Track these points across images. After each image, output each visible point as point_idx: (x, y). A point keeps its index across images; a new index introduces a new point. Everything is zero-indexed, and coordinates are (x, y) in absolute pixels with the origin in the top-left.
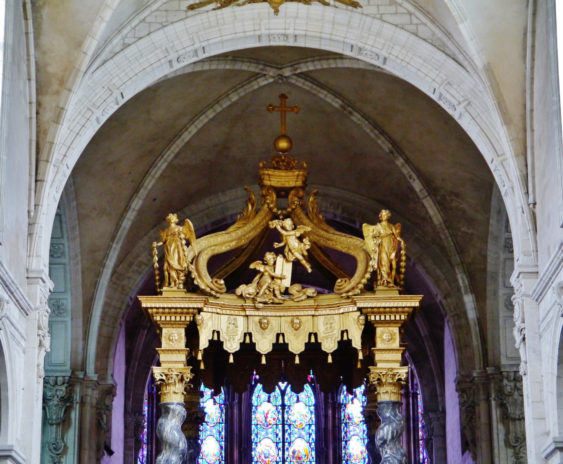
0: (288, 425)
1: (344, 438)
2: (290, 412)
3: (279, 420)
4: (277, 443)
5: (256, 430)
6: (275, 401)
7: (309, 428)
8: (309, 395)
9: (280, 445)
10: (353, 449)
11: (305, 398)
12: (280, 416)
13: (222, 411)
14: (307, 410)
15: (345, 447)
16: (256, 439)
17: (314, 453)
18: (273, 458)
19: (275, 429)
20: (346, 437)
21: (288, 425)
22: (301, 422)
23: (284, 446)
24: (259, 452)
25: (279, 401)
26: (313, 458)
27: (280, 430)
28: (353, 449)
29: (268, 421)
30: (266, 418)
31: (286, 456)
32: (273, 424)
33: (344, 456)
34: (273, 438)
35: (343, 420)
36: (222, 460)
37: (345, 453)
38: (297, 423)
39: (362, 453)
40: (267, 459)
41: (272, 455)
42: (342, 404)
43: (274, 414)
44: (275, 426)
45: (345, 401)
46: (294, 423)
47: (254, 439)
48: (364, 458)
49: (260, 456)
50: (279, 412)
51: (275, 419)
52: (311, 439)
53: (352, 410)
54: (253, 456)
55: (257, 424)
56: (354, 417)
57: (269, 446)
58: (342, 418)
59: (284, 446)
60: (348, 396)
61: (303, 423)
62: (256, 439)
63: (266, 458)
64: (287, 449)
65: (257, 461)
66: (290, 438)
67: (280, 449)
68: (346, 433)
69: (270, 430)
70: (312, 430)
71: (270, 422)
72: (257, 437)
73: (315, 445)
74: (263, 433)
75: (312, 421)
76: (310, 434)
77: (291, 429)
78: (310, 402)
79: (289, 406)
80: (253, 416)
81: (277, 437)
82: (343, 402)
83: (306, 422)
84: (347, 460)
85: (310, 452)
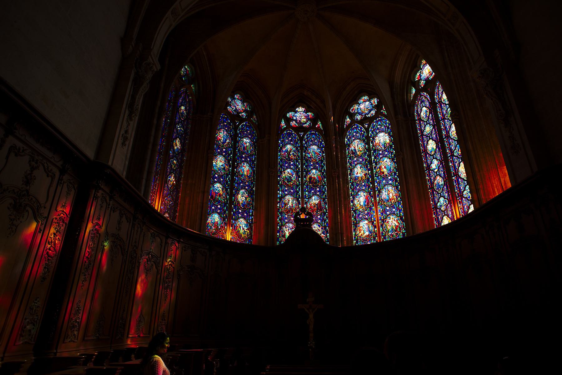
1: (349, 167)
3: (299, 157)
4: (297, 174)
9: (300, 174)
10: (357, 174)
12: (299, 154)
13: (255, 148)
15: (350, 174)
18: (294, 182)
19: (296, 163)
20: (351, 167)
23: (302, 174)
24: (283, 178)
25: (298, 144)
26: (325, 183)
28: (357, 174)
29: (290, 156)
30: (289, 154)
33: (350, 180)
35: (348, 155)
36: (254, 181)
37: (351, 178)
39: (365, 175)
42: (347, 144)
43: (295, 152)
45: (348, 142)
47: (279, 169)
48: (368, 179)
49: (284, 181)
50: (298, 151)
52: (323, 170)
53: (355, 148)
55: (282, 159)
56: (357, 151)
58: (347, 154)
59: (302, 174)
60: (351, 139)
61: (317, 159)
63: (288, 182)
64: (305, 177)
68: (350, 164)
69: (292, 163)
70: (324, 164)
74: (287, 165)
75: (324, 158)
76: (323, 167)
79: (306, 148)
82: (347, 143)
84: (353, 182)
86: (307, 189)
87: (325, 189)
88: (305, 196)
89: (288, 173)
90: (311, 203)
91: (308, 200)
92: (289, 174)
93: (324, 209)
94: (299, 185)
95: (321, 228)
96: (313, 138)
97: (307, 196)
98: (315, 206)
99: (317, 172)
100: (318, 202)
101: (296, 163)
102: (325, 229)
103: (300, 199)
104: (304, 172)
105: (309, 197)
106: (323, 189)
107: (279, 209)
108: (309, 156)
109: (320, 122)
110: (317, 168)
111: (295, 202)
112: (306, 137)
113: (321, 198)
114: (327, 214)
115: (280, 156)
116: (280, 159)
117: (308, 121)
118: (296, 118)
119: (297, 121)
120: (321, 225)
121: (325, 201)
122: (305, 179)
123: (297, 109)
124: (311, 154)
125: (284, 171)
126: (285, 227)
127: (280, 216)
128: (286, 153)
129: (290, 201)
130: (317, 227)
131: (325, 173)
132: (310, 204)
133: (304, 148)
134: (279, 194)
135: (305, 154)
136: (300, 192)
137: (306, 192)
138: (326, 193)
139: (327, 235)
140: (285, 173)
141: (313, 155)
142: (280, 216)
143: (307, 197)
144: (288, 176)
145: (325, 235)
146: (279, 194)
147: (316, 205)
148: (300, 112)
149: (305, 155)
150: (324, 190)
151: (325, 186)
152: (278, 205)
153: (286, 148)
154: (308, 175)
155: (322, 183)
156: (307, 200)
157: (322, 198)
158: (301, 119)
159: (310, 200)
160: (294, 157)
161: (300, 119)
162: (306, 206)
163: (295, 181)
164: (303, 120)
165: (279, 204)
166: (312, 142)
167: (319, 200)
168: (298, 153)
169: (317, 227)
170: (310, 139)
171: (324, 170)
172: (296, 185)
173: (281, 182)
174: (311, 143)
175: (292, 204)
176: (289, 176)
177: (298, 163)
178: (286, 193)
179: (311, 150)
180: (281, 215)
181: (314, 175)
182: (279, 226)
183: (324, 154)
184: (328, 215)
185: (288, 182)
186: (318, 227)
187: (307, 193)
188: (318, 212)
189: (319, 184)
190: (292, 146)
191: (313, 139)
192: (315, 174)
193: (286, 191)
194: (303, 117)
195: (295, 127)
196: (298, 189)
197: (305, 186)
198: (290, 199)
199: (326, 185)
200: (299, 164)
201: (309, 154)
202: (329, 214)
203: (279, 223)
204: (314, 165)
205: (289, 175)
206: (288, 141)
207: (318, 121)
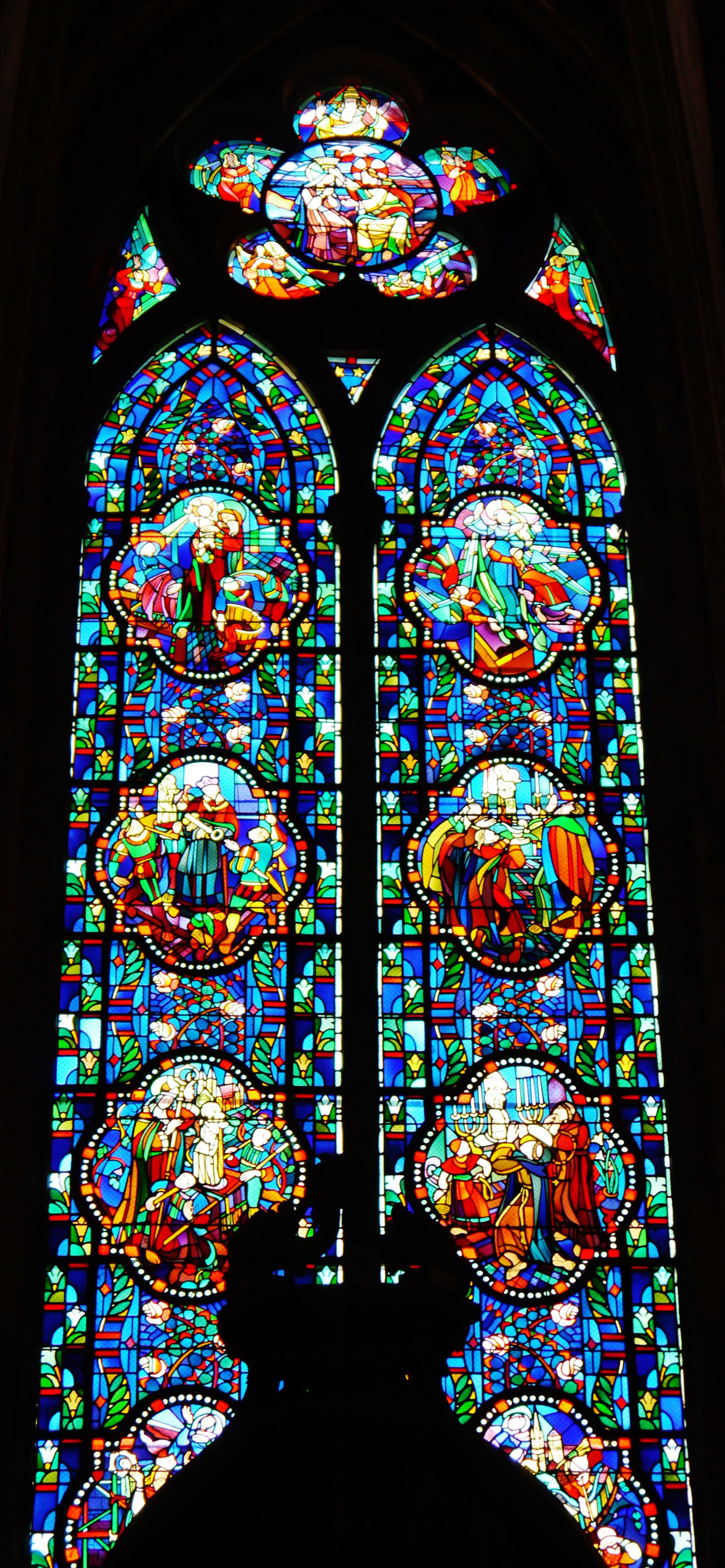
0: (396, 653)
2: (415, 563)
3: (323, 624)
5: (108, 694)
6: (284, 478)
7: (594, 684)
8: (579, 442)
11: (543, 467)
14: (565, 552)
16: (104, 759)
17: (638, 872)
18: (258, 906)
19: (284, 686)
21: (396, 653)
22: (522, 635)
24: (128, 865)
25: (318, 486)
26: (635, 912)
27: (329, 690)
29: (221, 623)
31: (381, 894)
32: (260, 644)
34: (257, 751)
38: (479, 643)
40: (208, 918)
41: (245, 881)
43: (280, 574)
44: (276, 666)
46: (453, 645)
47: (88, 759)
51: (290, 607)
52: (609, 765)
54: (70, 891)
55: (122, 646)
57: (231, 811)
61: (540, 642)
62: (104, 759)
63: (187, 906)
65: (109, 936)
66: (418, 751)
67: (326, 837)
69: (237, 692)
70: (622, 698)
71: (243, 635)
72: (114, 743)
73: (647, 809)
74: (174, 714)
75: (619, 631)
77: (432, 686)
78: (593, 497)
80: (90, 589)
81: (297, 746)
83: (564, 638)
85: (603, 863)
86: (413, 988)
87: (638, 984)
88: (399, 1059)
89: (195, 805)
90: (464, 1149)
91: (431, 1120)
92: (209, 817)
93: (625, 1226)
94: (315, 941)
95: (592, 1455)
96: (494, 413)
97: (415, 1063)
98: (512, 1186)
99: (543, 785)
100: (547, 1135)
101: (284, 686)
102: (641, 1469)
103: (324, 1109)
104: (386, 786)
105: (439, 1075)
106: (612, 974)
107: (64, 1228)
108: (445, 613)
109: (572, 251)
110: (545, 744)
111: (261, 1136)
112: (408, 408)
113: (585, 1089)
114: (662, 1276)
115: (96, 616)
116: (94, 647)
117: (429, 238)
118: (300, 209)
119: (308, 233)
120: (595, 1422)
121: (636, 1128)
122: (390, 870)
123: (305, 118)
124: (462, 590)
125: (140, 779)
126: (139, 1450)
127: (75, 1316)
128: (175, 588)
129: (210, 1132)
130: (538, 1444)
131: (631, 802)
132: (448, 1165)
133: (387, 528)
134: (76, 1051)
135: (399, 590)
136: (326, 1024)
137: (406, 1016)
138: (646, 1025)
139: (667, 1543)
140: (150, 806)
141: (492, 595)
142: (75, 1316)
143: (420, 1083)
144: (188, 836)
145: (644, 1539)
146: (76, 1051)
147: (536, 1167)
148: (338, 139)
149: (400, 607)
150: (621, 991)
151: (639, 953)
152: (59, 1182)
153: (170, 530)
154: (431, 826)
155: (605, 912)
156: (417, 1112)
157: (600, 1091)
158: (353, 216)
159: (453, 1114)
160: (268, 621)
161: (340, 221)
162: (408, 1184)
163: (269, 890)
164: (379, 226)
165: (66, 1163)
166: (479, 463)
167: (562, 1115)
168: (314, 585)
169: (538, 1444)
170: (459, 426)
171: (626, 763)
172: (291, 938)
173: (110, 909)
174: (470, 471)
175: (233, 1165)
176: (206, 841)
177: (305, 695)
178: (165, 1031)
179: (473, 545)
180: (87, 1300)
181: (508, 819)
182: (60, 1436)
183: (620, 594)
184: (675, 1297)
185: (187, 906)
186: (556, 1441)
187: (416, 1030)
188: (558, 1260)
189: (568, 924)
190: (241, 509)
191: (489, 428)
192: (510, 810)
193: (156, 1013)
194: (379, 198)
195: (280, 293)
196: (304, 989)
197: (392, 952)
198: (212, 1110)
199: (642, 938)
200: (325, 695)
201: (448, 593)
202: (684, 1285)
203: (57, 1401)
204: (507, 707)
205: (203, 830)
206: (199, 454)
207: (549, 233)
